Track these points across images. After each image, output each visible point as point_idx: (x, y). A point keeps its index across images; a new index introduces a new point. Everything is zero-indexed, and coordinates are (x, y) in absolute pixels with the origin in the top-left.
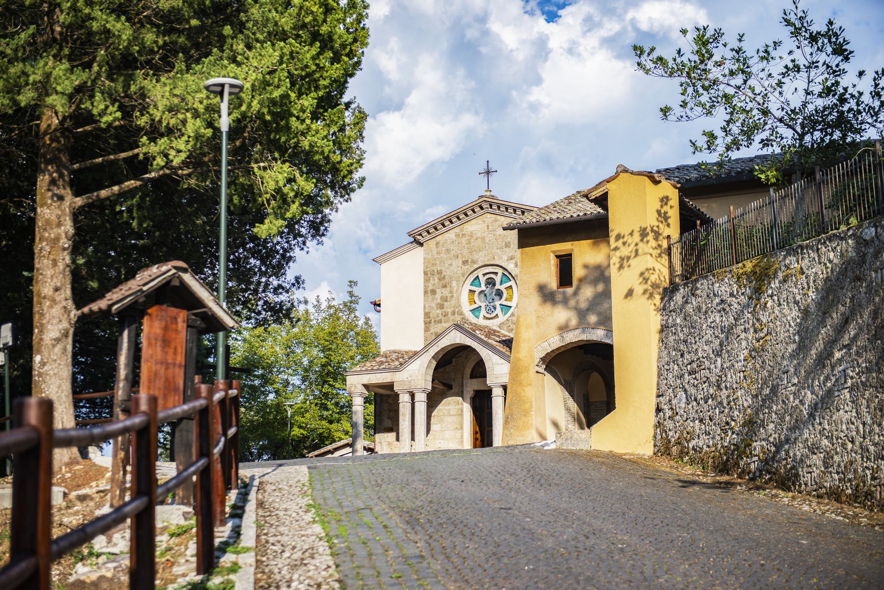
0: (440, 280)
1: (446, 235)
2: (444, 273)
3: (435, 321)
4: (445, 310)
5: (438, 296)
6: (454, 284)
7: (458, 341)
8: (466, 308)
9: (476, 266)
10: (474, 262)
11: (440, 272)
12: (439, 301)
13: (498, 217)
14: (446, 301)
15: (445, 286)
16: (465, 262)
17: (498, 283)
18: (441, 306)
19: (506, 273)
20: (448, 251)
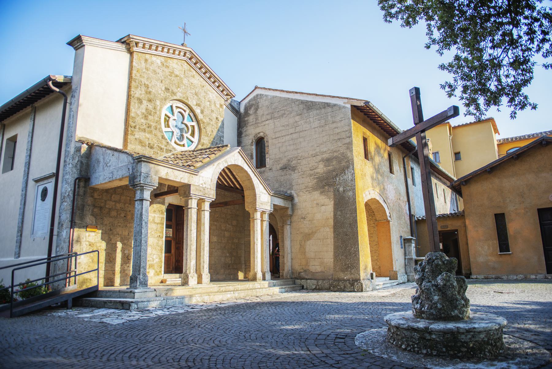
0: (146, 93)
1: (154, 58)
2: (150, 89)
3: (139, 129)
4: (148, 122)
5: (144, 106)
6: (158, 103)
7: (240, 164)
8: (164, 129)
9: (175, 98)
10: (174, 93)
11: (147, 86)
12: (144, 111)
13: (192, 69)
14: (150, 114)
15: (150, 101)
16: (167, 89)
17: (186, 118)
18: (146, 117)
19: (192, 114)
20: (155, 72)
